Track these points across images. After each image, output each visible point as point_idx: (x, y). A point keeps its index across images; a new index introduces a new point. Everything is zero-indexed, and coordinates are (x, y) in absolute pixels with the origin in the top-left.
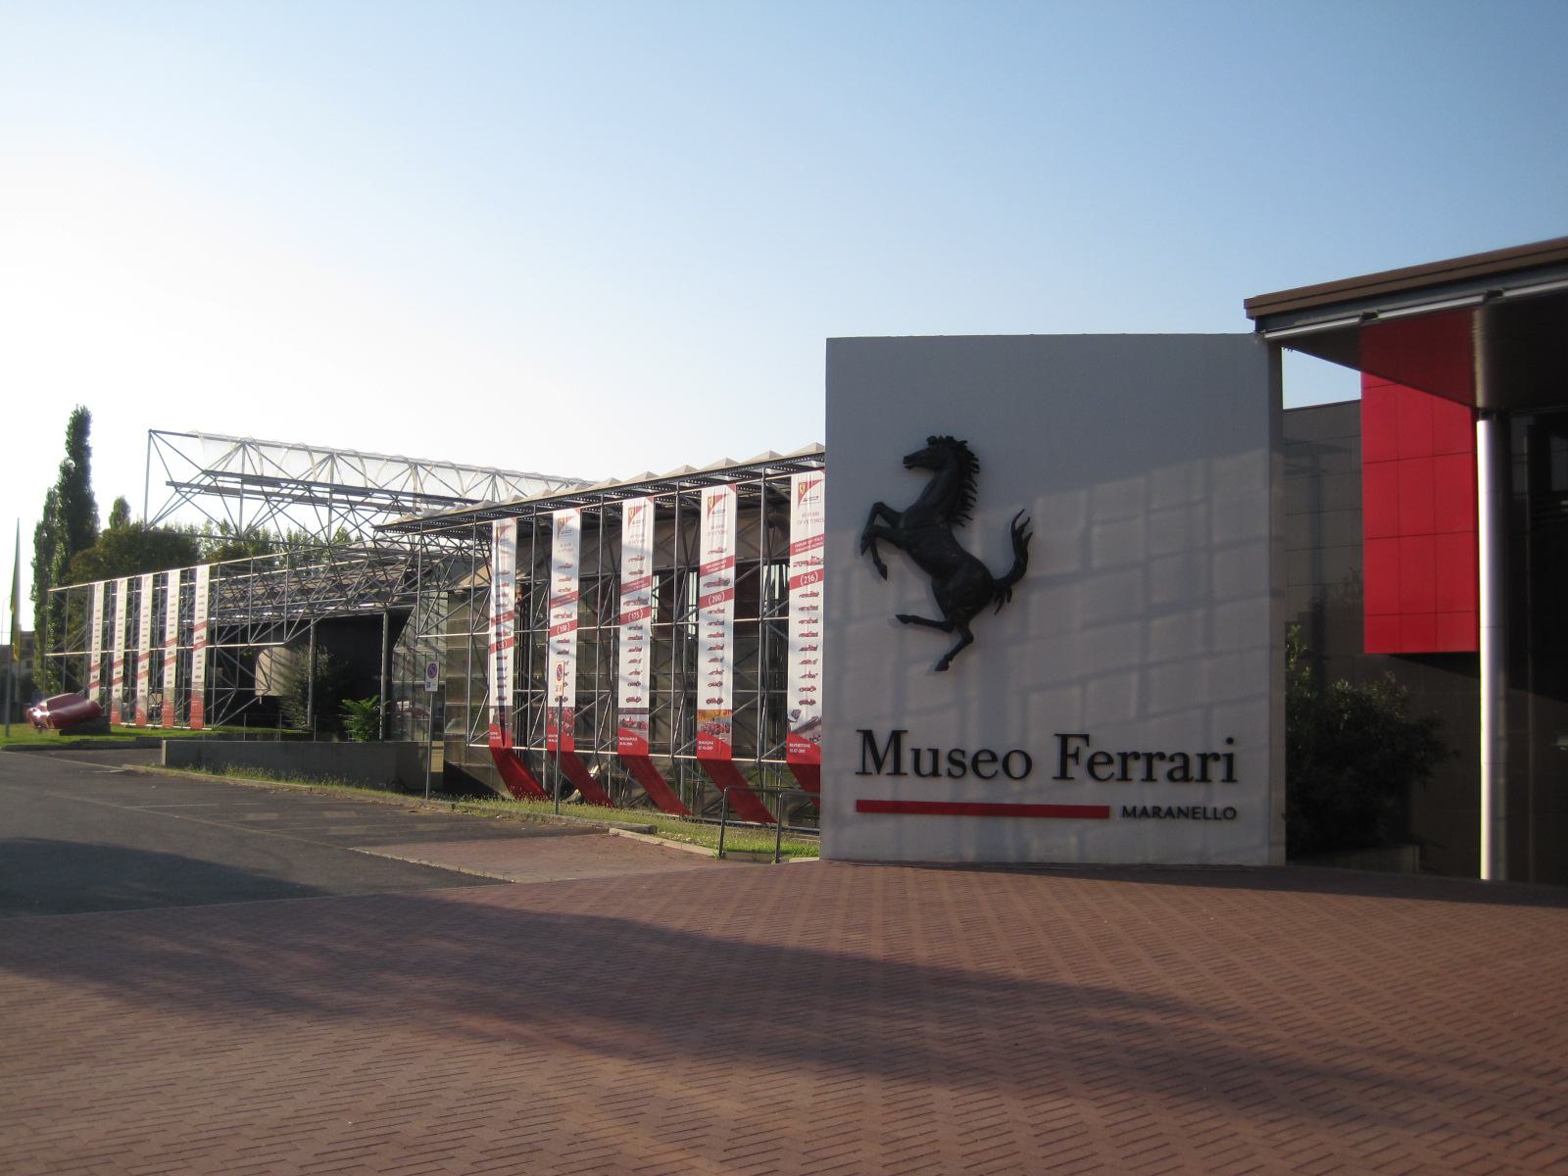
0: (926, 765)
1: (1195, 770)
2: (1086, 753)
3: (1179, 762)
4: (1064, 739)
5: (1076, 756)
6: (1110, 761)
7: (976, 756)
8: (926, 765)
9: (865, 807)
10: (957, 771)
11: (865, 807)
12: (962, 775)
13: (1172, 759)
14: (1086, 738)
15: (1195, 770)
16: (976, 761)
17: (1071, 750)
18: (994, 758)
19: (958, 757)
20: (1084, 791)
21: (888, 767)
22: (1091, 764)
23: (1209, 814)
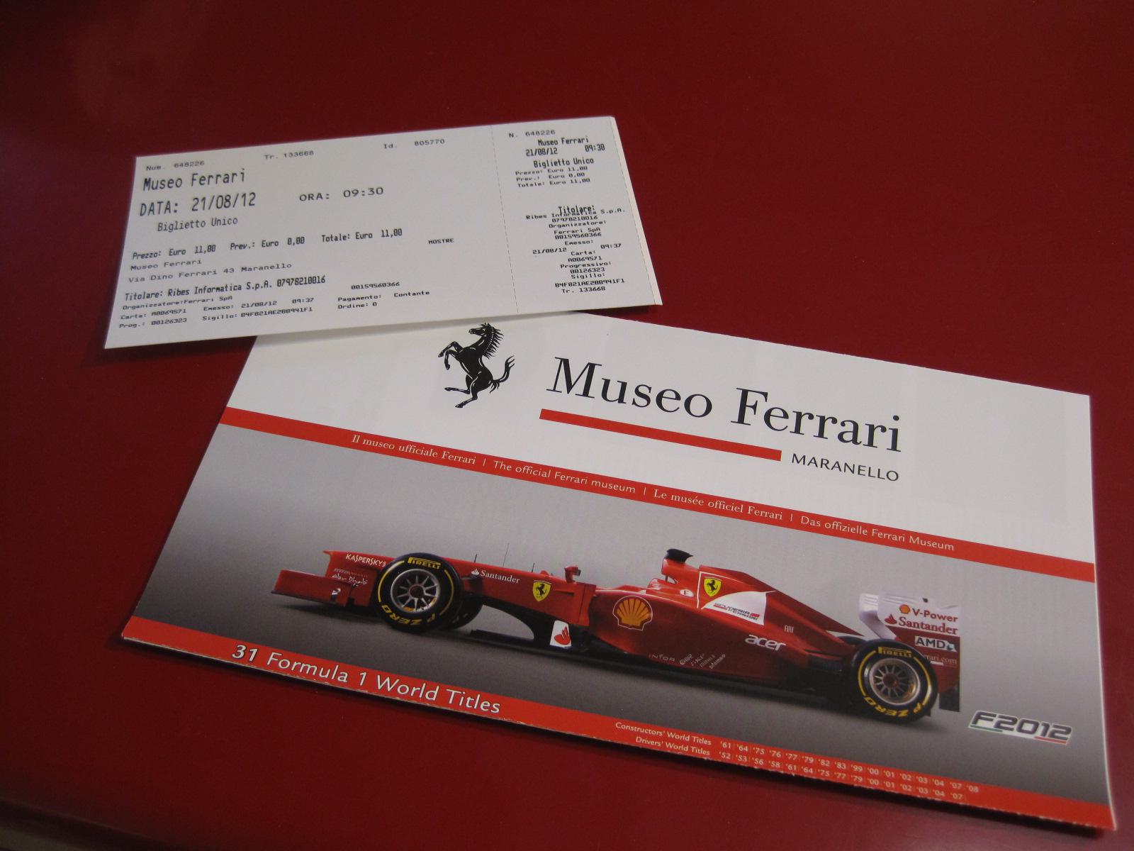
0: (614, 392)
1: (863, 435)
2: (763, 408)
3: (850, 427)
4: (745, 393)
5: (754, 407)
6: (786, 416)
7: (662, 393)
8: (614, 392)
9: (547, 415)
10: (642, 402)
11: (547, 415)
12: (646, 406)
13: (843, 424)
14: (765, 395)
15: (863, 435)
16: (660, 398)
17: (750, 402)
18: (678, 397)
19: (643, 390)
20: (755, 433)
21: (579, 387)
22: (768, 416)
23: (874, 473)
